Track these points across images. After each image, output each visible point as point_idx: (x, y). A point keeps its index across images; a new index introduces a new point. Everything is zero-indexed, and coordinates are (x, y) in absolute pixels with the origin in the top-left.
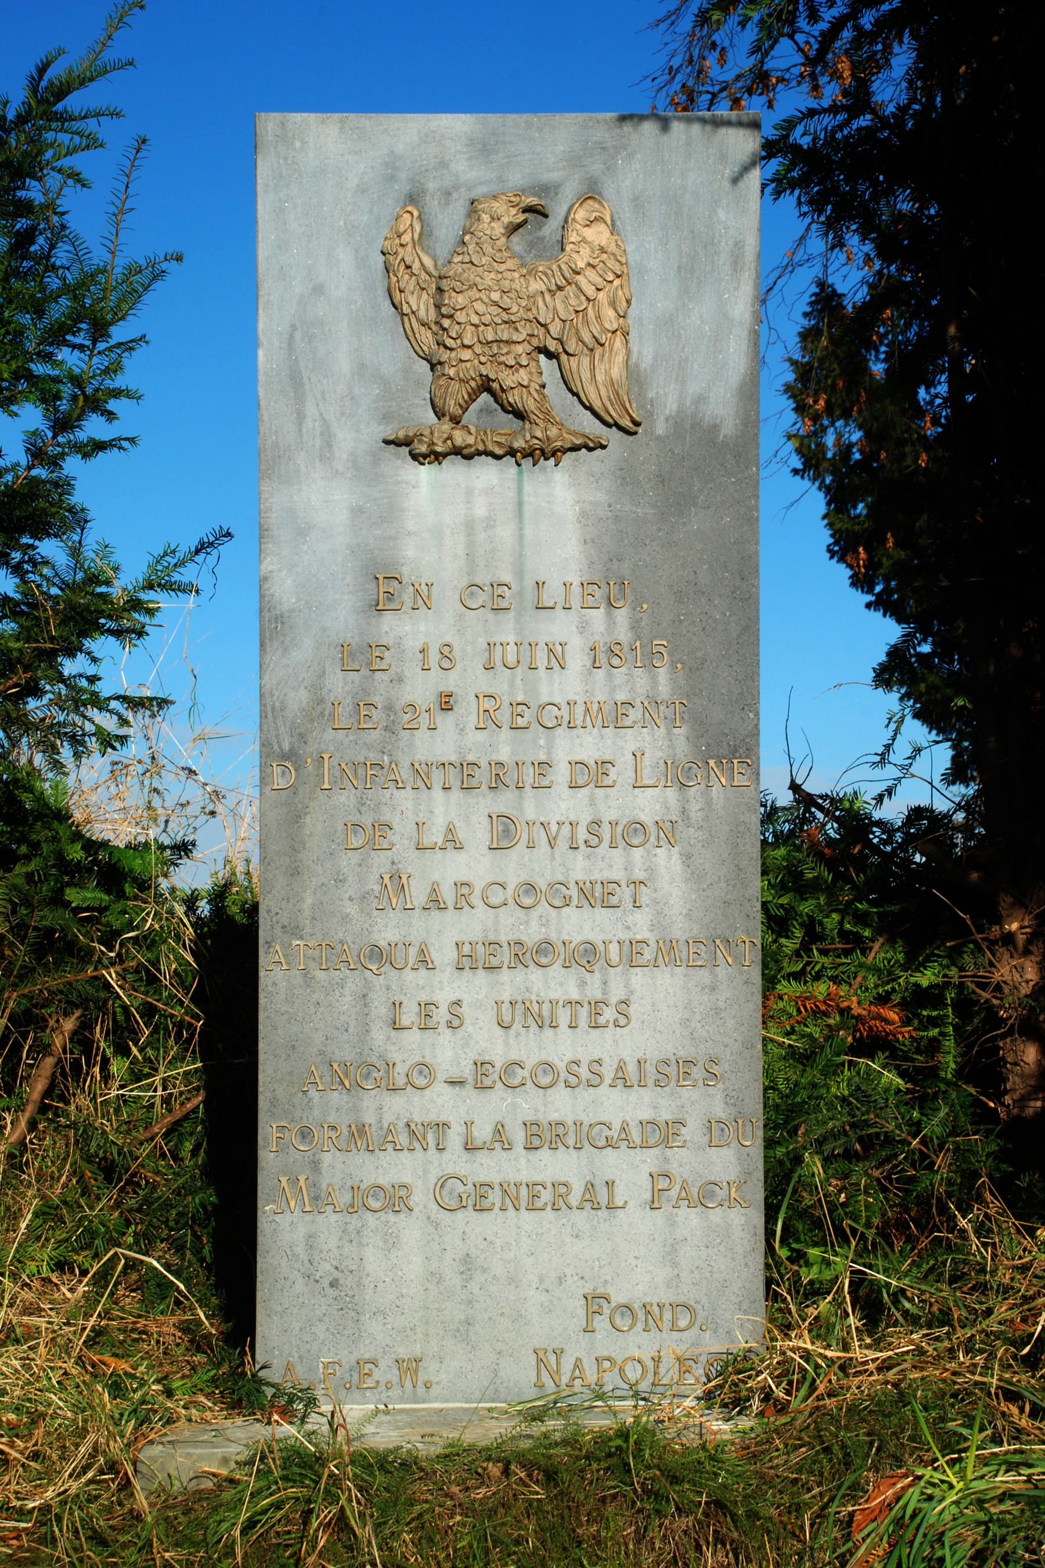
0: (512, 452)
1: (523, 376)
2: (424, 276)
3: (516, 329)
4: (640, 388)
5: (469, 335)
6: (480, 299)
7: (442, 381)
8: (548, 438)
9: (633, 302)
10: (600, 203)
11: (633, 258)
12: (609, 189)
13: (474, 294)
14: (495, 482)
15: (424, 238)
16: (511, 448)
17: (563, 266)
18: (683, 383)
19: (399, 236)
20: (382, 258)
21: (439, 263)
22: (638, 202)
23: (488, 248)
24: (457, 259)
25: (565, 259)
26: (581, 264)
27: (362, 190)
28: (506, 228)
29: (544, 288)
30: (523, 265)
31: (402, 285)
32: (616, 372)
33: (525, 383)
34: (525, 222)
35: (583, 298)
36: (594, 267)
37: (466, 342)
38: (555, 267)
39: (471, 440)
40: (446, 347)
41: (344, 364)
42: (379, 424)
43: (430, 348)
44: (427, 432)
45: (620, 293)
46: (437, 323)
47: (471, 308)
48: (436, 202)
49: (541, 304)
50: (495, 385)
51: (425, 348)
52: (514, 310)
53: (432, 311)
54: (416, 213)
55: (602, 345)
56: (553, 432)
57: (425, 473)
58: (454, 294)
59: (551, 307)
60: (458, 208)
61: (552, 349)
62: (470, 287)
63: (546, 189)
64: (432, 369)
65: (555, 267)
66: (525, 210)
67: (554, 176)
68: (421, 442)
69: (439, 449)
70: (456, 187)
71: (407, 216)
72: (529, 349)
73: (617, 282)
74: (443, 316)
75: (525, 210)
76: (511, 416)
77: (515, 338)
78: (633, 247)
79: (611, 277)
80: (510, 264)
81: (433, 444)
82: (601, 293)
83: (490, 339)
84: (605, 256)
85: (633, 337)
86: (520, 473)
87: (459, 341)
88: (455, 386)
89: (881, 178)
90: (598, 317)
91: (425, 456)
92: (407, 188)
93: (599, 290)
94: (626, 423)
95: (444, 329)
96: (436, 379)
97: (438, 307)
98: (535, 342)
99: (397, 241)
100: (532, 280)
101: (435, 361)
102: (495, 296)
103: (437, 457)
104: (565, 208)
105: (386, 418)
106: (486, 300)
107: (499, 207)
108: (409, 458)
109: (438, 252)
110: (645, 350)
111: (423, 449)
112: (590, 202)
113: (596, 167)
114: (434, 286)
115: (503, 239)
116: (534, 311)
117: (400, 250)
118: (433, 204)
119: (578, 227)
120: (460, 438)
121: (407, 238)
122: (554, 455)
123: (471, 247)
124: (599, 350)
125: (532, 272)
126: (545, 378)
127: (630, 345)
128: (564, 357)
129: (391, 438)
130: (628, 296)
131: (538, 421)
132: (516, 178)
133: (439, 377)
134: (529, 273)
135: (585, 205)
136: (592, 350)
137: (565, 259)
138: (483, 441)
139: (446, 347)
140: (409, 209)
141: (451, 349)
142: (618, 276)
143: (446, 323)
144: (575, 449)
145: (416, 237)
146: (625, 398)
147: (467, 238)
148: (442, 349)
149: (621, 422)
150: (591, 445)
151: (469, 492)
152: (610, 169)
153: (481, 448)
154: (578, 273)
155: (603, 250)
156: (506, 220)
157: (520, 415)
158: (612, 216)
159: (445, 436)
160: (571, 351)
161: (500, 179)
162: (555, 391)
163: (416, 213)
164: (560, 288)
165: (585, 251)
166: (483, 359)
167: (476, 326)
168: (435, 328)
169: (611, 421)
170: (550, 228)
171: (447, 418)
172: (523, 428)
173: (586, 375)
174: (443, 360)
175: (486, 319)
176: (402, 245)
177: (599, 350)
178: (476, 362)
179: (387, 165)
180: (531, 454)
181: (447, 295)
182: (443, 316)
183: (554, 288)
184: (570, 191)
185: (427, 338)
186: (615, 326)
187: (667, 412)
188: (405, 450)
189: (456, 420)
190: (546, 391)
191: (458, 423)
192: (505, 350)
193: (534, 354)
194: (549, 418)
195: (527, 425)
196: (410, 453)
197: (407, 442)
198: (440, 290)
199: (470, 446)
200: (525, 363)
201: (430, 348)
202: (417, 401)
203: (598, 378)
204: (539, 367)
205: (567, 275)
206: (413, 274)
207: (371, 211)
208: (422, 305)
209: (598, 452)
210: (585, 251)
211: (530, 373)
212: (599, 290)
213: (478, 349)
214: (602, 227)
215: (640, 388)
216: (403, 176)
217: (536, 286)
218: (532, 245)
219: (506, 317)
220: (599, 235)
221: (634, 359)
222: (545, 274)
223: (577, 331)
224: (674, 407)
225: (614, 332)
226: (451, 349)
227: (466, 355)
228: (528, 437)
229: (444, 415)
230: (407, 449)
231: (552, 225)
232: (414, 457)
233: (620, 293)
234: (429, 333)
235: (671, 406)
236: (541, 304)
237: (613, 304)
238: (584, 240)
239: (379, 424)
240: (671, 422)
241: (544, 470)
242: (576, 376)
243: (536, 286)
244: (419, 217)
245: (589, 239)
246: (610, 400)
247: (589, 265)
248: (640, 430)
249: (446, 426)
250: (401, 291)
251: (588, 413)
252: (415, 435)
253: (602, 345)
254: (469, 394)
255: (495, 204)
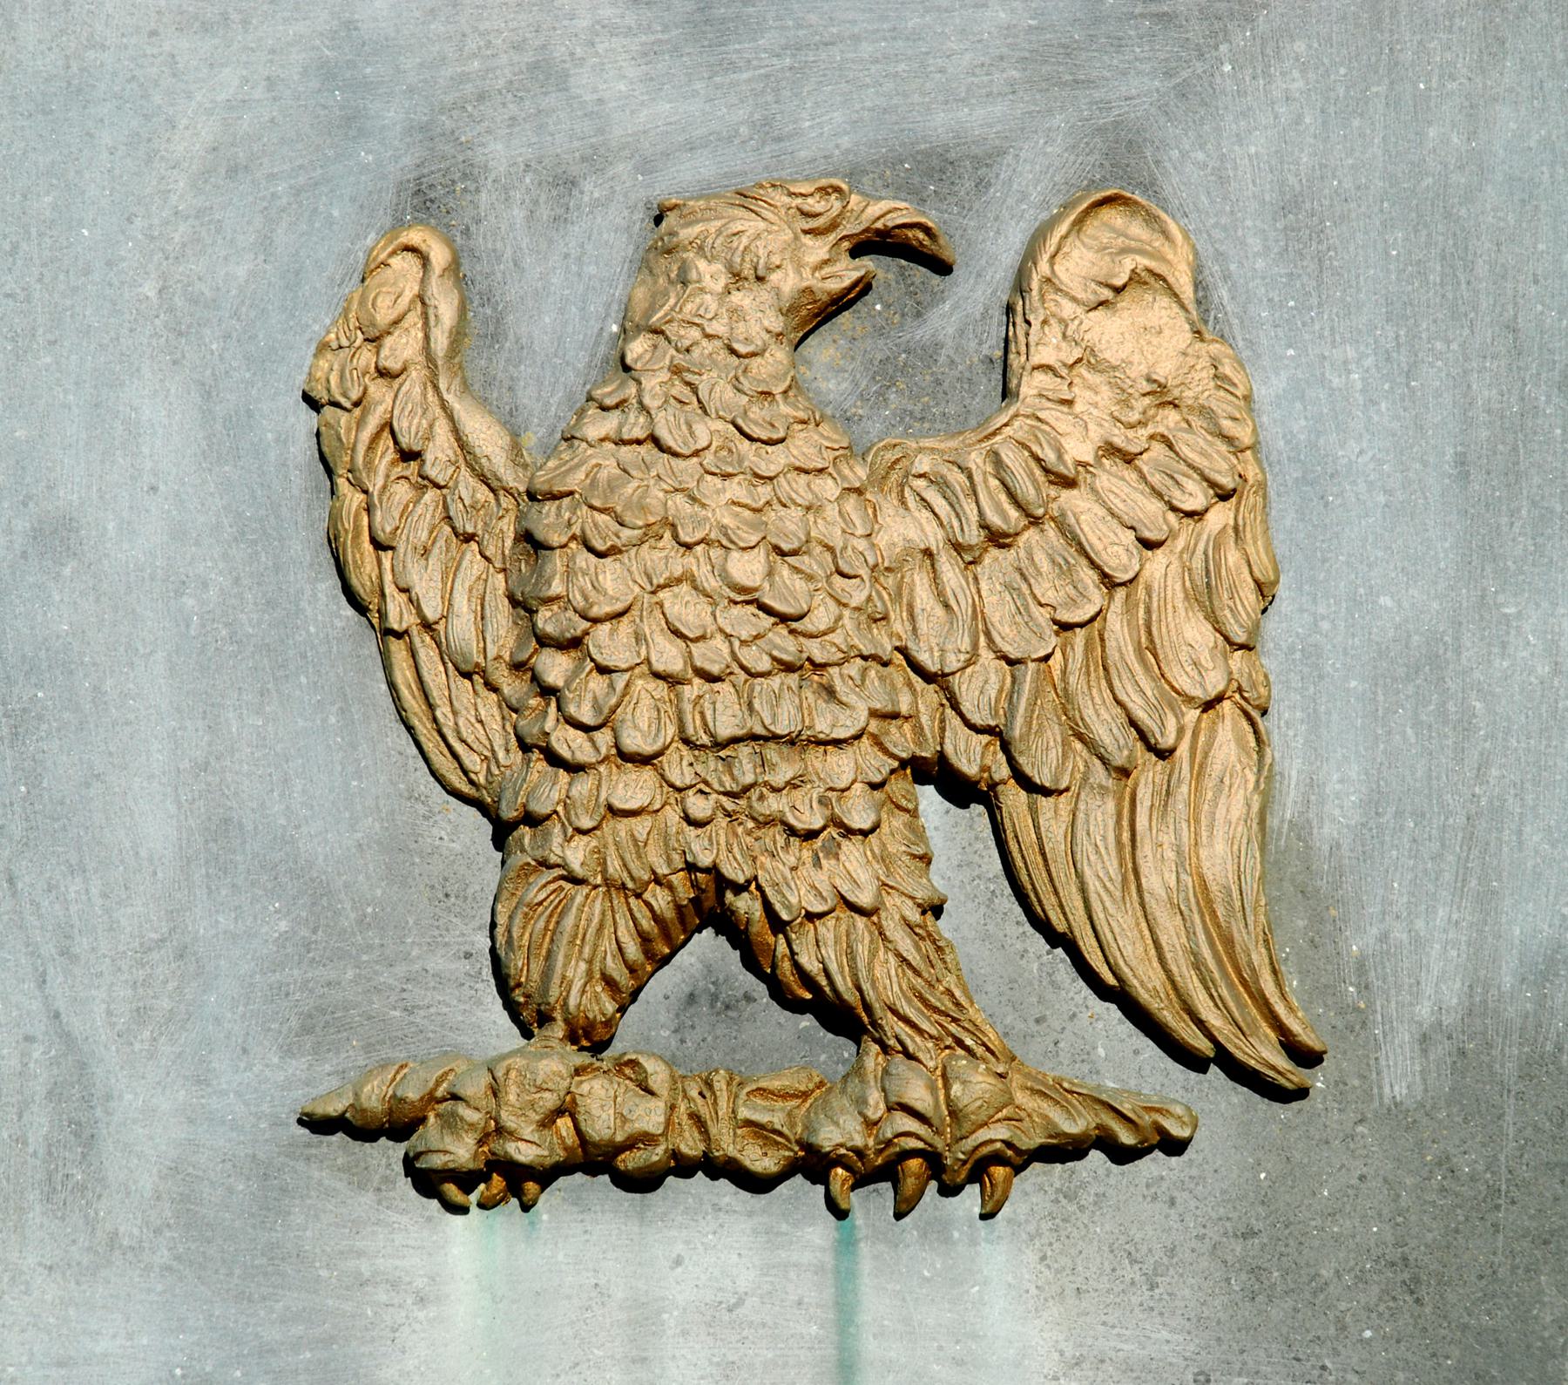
0: (813, 1164)
1: (855, 868)
2: (468, 487)
3: (830, 692)
4: (1317, 919)
5: (644, 716)
6: (688, 578)
7: (538, 889)
8: (954, 1113)
9: (1282, 591)
10: (1151, 219)
11: (1280, 425)
12: (1183, 169)
13: (662, 558)
14: (746, 1278)
15: (472, 346)
16: (809, 1148)
17: (1010, 456)
18: (1486, 900)
19: (375, 340)
20: (309, 419)
21: (530, 439)
22: (1300, 219)
23: (717, 388)
24: (598, 426)
25: (1019, 429)
26: (1079, 449)
27: (229, 165)
28: (789, 311)
29: (934, 537)
30: (852, 452)
31: (385, 524)
32: (1220, 857)
33: (865, 899)
34: (863, 287)
35: (1088, 576)
36: (1129, 459)
37: (634, 742)
38: (976, 460)
39: (649, 1116)
40: (554, 759)
41: (153, 823)
42: (288, 1052)
43: (490, 758)
44: (475, 1087)
45: (1233, 557)
46: (518, 667)
47: (650, 615)
48: (519, 214)
49: (923, 596)
50: (746, 905)
51: (472, 761)
52: (820, 619)
53: (502, 618)
54: (439, 255)
55: (1164, 754)
56: (975, 1085)
57: (469, 1242)
58: (584, 559)
59: (963, 608)
60: (607, 234)
61: (970, 769)
62: (650, 534)
63: (937, 168)
64: (499, 841)
65: (976, 460)
66: (861, 247)
67: (979, 119)
68: (451, 1123)
69: (523, 1153)
70: (596, 160)
71: (405, 265)
72: (877, 765)
73: (1220, 516)
74: (544, 641)
75: (861, 247)
76: (807, 1021)
77: (823, 726)
78: (1279, 383)
79: (1195, 496)
80: (805, 447)
81: (500, 1131)
82: (1159, 558)
83: (725, 730)
84: (1172, 417)
85: (1281, 725)
86: (846, 1246)
87: (604, 738)
88: (587, 907)
89: (1263, 1176)
90: (1149, 649)
91: (467, 1180)
92: (404, 161)
93: (1149, 545)
94: (1265, 1053)
95: (547, 691)
96: (513, 878)
97: (523, 605)
98: (902, 741)
99: (366, 357)
100: (889, 506)
101: (509, 813)
102: (748, 568)
103: (522, 1183)
104: (1014, 240)
105: (316, 1027)
106: (712, 583)
107: (762, 233)
108: (405, 1185)
109: (526, 397)
110: (1331, 769)
111: (462, 1152)
112: (1113, 217)
113: (1134, 86)
114: (508, 528)
115: (779, 354)
116: (899, 625)
117: (378, 389)
118: (504, 222)
119: (1068, 309)
120: (607, 1108)
121: (402, 348)
122: (979, 1170)
123: (654, 384)
124: (1150, 774)
125: (892, 478)
126: (941, 879)
127: (1273, 753)
128: (1014, 799)
129: (334, 1108)
130: (1264, 571)
131: (914, 1042)
132: (828, 127)
133: (526, 871)
134: (879, 479)
135: (1092, 227)
136: (1124, 772)
137: (1019, 429)
138: (697, 1119)
139: (554, 759)
140: (414, 237)
141: (575, 768)
142: (1224, 496)
143: (555, 668)
144: (1063, 1151)
145: (440, 342)
146: (1259, 958)
147: (637, 348)
148: (539, 765)
149: (1241, 1050)
150: (1127, 1138)
151: (643, 1320)
152: (1189, 95)
153: (691, 1146)
154: (1069, 483)
155: (1163, 397)
156: (788, 282)
157: (844, 1018)
158: (1197, 270)
159: (550, 1101)
160: (1044, 777)
161: (765, 129)
162: (986, 938)
163: (439, 255)
164: (998, 539)
165: (1094, 398)
166: (699, 806)
167: (672, 681)
168: (513, 686)
169: (1203, 1045)
170: (960, 311)
171: (558, 1030)
172: (858, 1070)
173: (1102, 868)
174: (540, 808)
175: (713, 655)
176: (383, 373)
177: (1150, 774)
178: (672, 816)
179: (328, 74)
180: (889, 1172)
181: (557, 561)
182: (544, 641)
183: (974, 536)
184: (1036, 173)
185: (479, 723)
186: (1215, 683)
187: (1424, 1011)
188: (390, 1153)
189: (591, 1038)
190: (944, 926)
191: (598, 1048)
192: (784, 772)
193: (899, 787)
194: (959, 1038)
195: (873, 1057)
196: (409, 1163)
197: (398, 1124)
198: (532, 543)
199: (647, 1139)
200: (860, 821)
201: (490, 758)
202: (438, 962)
203: (1151, 881)
204: (918, 833)
205: (1027, 490)
206: (426, 482)
207: (265, 244)
208: (462, 598)
209: (1155, 1165)
210: (1094, 398)
211: (884, 859)
212: (1149, 545)
213: (679, 768)
214: (1160, 311)
215: (1317, 919)
216: (391, 114)
217: (904, 528)
218: (886, 374)
219: (786, 645)
220: (1147, 339)
221: (1288, 807)
222: (942, 485)
223: (1066, 701)
224: (1452, 995)
225: (1208, 706)
226: (575, 768)
227: (633, 788)
228: (876, 1105)
229: (544, 1019)
230: (398, 1151)
231: (972, 295)
232: (427, 1182)
233: (1233, 557)
234: (488, 705)
235: (1433, 987)
236: (923, 596)
237: (1205, 597)
238: (1089, 359)
239: (288, 1052)
240: (1440, 1049)
241: (940, 1232)
242: (1061, 870)
243: (904, 528)
244: (454, 267)
245: (1110, 355)
246: (1198, 965)
247: (1111, 450)
248: (1318, 1080)
249: (553, 1062)
250: (378, 546)
251: (1112, 1012)
252: (431, 1099)
253: (1164, 754)
254: (644, 939)
255: (749, 225)
